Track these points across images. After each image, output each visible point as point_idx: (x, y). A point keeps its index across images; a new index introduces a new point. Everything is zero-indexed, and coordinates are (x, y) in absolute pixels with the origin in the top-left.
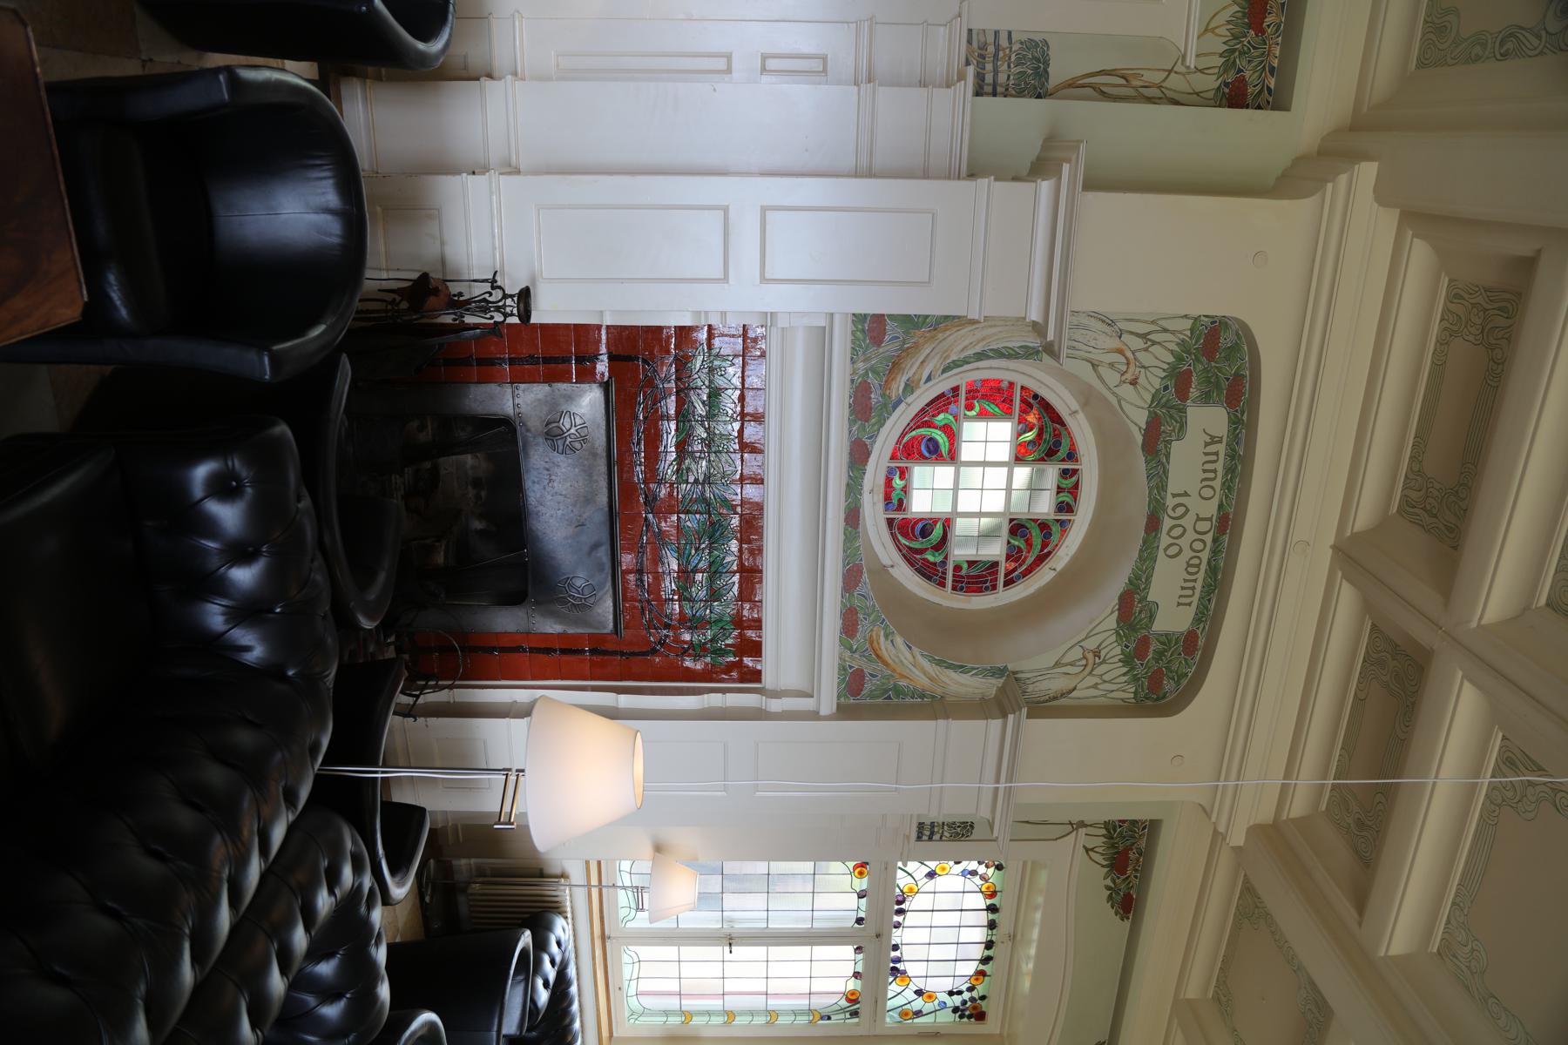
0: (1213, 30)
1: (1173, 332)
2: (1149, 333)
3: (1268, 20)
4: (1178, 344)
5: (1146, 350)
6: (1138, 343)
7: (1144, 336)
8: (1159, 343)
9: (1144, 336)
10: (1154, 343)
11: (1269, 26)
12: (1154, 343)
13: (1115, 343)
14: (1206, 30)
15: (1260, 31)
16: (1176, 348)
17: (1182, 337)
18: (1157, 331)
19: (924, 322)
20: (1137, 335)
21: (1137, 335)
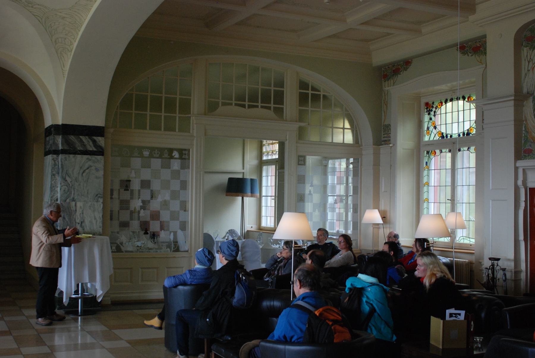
0: (481, 60)
1: (527, 53)
2: (528, 61)
3: (478, 45)
4: (530, 50)
5: (532, 60)
6: (531, 64)
7: (529, 62)
8: (530, 57)
9: (529, 62)
10: (530, 58)
11: (479, 44)
12: (530, 58)
13: (531, 71)
14: (481, 62)
15: (480, 47)
16: (531, 50)
17: (528, 50)
18: (527, 58)
19: (526, 136)
20: (529, 64)
21: (529, 64)
